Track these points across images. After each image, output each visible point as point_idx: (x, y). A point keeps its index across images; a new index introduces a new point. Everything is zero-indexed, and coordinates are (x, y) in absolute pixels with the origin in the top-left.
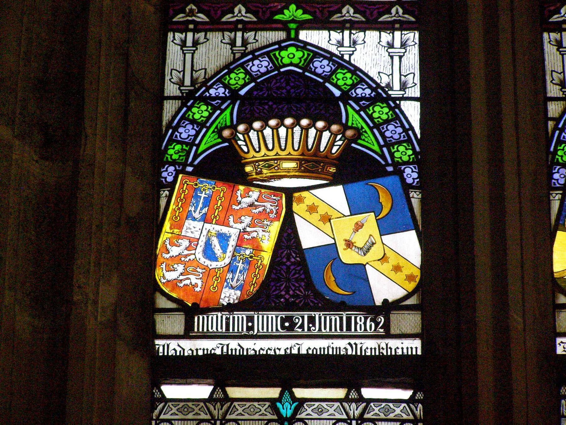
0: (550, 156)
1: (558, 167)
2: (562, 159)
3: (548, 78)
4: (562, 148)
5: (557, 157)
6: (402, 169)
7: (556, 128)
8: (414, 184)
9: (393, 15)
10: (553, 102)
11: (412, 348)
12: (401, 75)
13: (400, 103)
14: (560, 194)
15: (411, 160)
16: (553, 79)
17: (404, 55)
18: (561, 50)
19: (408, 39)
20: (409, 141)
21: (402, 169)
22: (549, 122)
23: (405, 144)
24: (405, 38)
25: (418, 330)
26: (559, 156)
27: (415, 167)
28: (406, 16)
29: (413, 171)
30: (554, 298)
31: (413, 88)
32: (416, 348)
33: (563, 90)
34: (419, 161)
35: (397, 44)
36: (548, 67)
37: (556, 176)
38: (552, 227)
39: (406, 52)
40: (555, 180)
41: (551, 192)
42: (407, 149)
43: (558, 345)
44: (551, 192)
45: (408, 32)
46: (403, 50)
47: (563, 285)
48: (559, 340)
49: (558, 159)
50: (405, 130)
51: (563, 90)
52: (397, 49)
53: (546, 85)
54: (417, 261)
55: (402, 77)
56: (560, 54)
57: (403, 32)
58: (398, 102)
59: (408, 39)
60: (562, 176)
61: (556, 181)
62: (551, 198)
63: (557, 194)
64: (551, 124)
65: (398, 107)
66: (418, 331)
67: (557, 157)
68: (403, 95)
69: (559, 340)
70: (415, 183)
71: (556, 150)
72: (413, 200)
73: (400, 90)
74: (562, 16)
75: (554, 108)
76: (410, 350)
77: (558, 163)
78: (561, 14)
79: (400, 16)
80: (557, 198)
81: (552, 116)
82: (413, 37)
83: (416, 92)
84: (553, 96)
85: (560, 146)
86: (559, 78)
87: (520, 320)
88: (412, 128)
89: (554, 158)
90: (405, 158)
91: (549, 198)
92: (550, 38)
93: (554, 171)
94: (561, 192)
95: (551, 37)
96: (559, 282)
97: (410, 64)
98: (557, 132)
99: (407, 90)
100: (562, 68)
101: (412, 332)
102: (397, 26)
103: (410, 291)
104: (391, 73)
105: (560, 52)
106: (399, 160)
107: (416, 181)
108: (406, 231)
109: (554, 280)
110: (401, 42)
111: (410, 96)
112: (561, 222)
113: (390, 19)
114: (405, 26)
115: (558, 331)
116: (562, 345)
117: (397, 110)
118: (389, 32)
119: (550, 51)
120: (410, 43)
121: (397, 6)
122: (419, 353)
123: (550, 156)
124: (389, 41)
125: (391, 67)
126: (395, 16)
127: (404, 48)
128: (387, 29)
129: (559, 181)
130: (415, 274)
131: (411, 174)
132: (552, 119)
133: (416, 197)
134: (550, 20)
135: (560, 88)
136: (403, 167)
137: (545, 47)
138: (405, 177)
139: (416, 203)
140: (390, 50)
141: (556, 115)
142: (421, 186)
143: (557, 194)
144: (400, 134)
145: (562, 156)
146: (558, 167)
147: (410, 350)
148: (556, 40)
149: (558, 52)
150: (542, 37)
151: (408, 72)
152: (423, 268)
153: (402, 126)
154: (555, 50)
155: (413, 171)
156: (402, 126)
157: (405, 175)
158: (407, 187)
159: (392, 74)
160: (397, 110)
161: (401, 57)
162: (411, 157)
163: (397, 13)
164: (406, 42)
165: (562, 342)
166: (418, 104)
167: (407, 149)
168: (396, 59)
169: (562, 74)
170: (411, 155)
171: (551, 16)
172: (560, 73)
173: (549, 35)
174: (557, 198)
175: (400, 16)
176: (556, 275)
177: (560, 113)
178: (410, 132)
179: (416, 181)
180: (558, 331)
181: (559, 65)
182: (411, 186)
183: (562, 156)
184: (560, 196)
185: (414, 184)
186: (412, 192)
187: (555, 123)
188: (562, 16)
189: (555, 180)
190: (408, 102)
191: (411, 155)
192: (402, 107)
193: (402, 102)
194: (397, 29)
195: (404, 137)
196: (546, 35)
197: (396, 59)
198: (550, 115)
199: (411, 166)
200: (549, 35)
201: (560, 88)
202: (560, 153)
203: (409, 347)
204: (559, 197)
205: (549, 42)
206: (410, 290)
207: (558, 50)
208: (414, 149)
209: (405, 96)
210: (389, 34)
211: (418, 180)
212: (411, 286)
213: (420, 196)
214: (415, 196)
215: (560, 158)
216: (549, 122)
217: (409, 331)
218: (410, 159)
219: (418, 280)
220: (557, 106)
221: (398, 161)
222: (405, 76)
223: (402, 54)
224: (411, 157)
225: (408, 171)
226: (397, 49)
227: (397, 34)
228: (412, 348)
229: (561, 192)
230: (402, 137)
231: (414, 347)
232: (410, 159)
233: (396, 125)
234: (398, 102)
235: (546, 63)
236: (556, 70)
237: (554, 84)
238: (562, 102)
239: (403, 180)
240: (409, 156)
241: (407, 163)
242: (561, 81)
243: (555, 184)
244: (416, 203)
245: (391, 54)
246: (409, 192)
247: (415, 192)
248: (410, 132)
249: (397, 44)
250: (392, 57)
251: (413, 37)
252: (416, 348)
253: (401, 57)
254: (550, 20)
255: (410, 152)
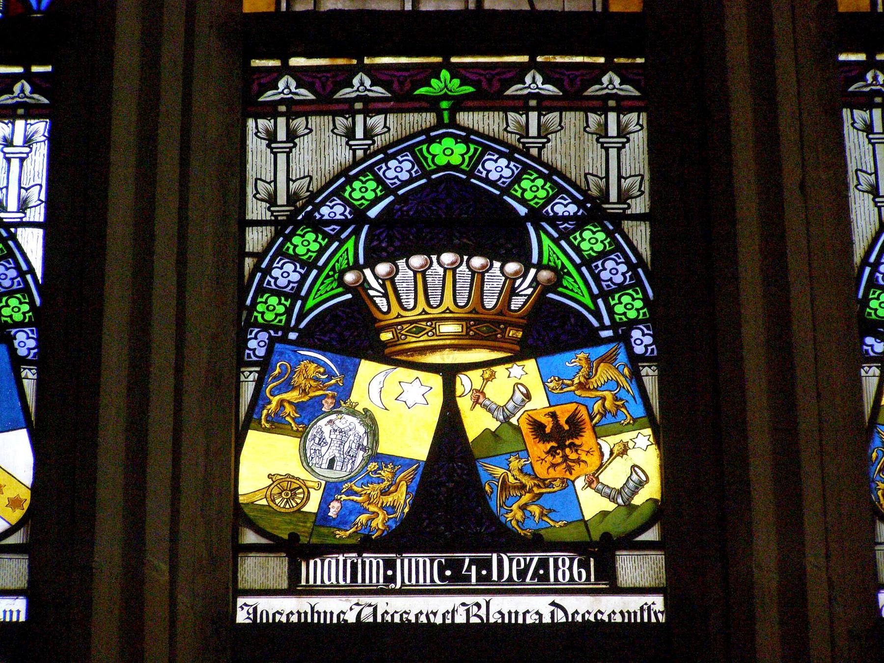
0: (245, 314)
1: (256, 330)
2: (262, 317)
3: (250, 190)
4: (263, 300)
5: (255, 314)
6: (12, 333)
7: (256, 268)
8: (29, 357)
9: (15, 94)
10: (255, 228)
11: (11, 612)
12: (20, 188)
13: (16, 231)
14: (256, 371)
15: (27, 320)
16: (258, 192)
17: (28, 156)
18: (273, 145)
19: (36, 132)
20: (26, 290)
21: (12, 333)
22: (247, 259)
23: (19, 296)
24: (31, 129)
25: (22, 583)
26: (258, 312)
27: (32, 331)
28: (36, 96)
29: (28, 338)
30: (236, 535)
31: (38, 208)
32: (18, 612)
33: (272, 209)
34: (39, 320)
35: (18, 140)
36: (251, 173)
37: (252, 344)
38: (241, 423)
39: (31, 151)
40: (250, 350)
41: (242, 369)
42: (21, 303)
43: (239, 609)
44: (242, 369)
45: (36, 121)
46: (27, 150)
47: (251, 514)
48: (241, 601)
49: (256, 317)
50: (21, 274)
51: (272, 209)
52: (19, 149)
53: (245, 200)
54: (27, 477)
55: (22, 190)
56: (272, 152)
57: (29, 121)
58: (13, 230)
59: (36, 132)
60: (262, 344)
61: (251, 352)
62: (242, 378)
63: (251, 372)
64: (249, 262)
65: (13, 237)
66: (22, 586)
67: (255, 314)
68: (21, 218)
69: (241, 601)
70: (32, 355)
71: (254, 303)
72: (25, 381)
73: (18, 212)
74: (280, 93)
75: (255, 238)
76: (8, 614)
77: (256, 324)
78: (278, 88)
79: (26, 97)
80: (251, 378)
81: (251, 250)
82: (40, 127)
83: (37, 214)
84: (255, 218)
85: (262, 297)
86: (266, 189)
87: (165, 567)
88: (31, 271)
89: (250, 314)
90: (18, 317)
91: (239, 378)
92: (257, 127)
93: (249, 337)
94: (258, 369)
95: (260, 126)
96: (246, 510)
97: (36, 170)
98: (259, 274)
99: (28, 211)
100: (272, 174)
101: (13, 587)
102: (21, 111)
103: (14, 523)
104: (5, 185)
105: (350, 146)
106: (8, 320)
107: (33, 352)
108: (12, 430)
109: (238, 507)
110: (25, 137)
111: (32, 220)
112: (255, 416)
113: (10, 102)
114: (31, 112)
115: (240, 586)
116: (246, 608)
117: (10, 243)
118: (6, 121)
119: (256, 146)
120: (39, 137)
121: (23, 81)
122: (22, 618)
123: (245, 314)
124: (7, 135)
125: (6, 175)
126: (18, 97)
127: (29, 146)
128: (5, 117)
129: (257, 353)
130: (23, 497)
131: (25, 342)
132: (251, 255)
133: (29, 378)
134: (260, 100)
135: (268, 205)
136: (13, 331)
137: (249, 142)
138: (16, 345)
139: (29, 387)
140: (6, 150)
141: (259, 249)
142: (41, 362)
143: (251, 372)
144: (12, 279)
145: (263, 313)
146: (256, 330)
147: (8, 614)
148: (267, 131)
149: (269, 150)
150: (244, 126)
151: (32, 183)
152: (35, 489)
153: (18, 267)
154: (344, 143)
155: (28, 338)
156: (18, 267)
157: (16, 343)
158: (17, 362)
159: (7, 187)
160: (10, 243)
161: (22, 160)
162: (27, 315)
163: (22, 91)
164: (33, 136)
165: (245, 605)
166: (39, 232)
167: (21, 303)
168: (15, 163)
169: (272, 184)
170: (28, 312)
171: (261, 93)
172: (269, 183)
173: (256, 123)
174: (251, 378)
175: (26, 97)
176: (242, 500)
177: (265, 245)
178: (29, 277)
179: (33, 352)
180: (240, 586)
181: (268, 169)
182: (24, 361)
183: (263, 313)
184: (257, 375)
185: (29, 357)
186: (25, 369)
187: (255, 260)
188: (280, 93)
189: (250, 350)
190: (29, 230)
191: (28, 312)
192: (19, 238)
193: (20, 230)
194: (21, 117)
195: (19, 284)
196: (251, 123)
197: (15, 163)
198: (249, 248)
199: (26, 329)
200: (256, 123)
201: (268, 205)
202: (260, 308)
203: (8, 610)
204: (254, 376)
205: (256, 134)
206: (14, 522)
207: (268, 146)
208: (32, 303)
209: (24, 220)
210: (7, 124)
211: (36, 351)
212: (18, 514)
213: (35, 377)
214: (30, 375)
215: (259, 316)
216: (247, 259)
217: (9, 586)
218: (25, 318)
219: (26, 506)
220: (260, 234)
221: (6, 322)
222: (27, 190)
223: (25, 155)
224: (27, 315)
225: (21, 336)
226: (19, 149)
227: (20, 124)
228: (11, 612)
229: (258, 369)
230: (16, 284)
231: (14, 609)
232: (25, 318)
233: (8, 266)
234: (13, 230)
235: (249, 166)
236: (263, 178)
237: (257, 199)
238: (269, 228)
239: (12, 351)
240: (24, 313)
241: (20, 325)
242: (269, 194)
243: (249, 356)
244: (29, 387)
245: (7, 156)
246: (20, 368)
247: (30, 369)
248: (29, 277)
249: (18, 140)
250: (8, 160)
251: (40, 127)
252: (18, 612)
253: (22, 160)
254: (260, 100)
255: (26, 308)
